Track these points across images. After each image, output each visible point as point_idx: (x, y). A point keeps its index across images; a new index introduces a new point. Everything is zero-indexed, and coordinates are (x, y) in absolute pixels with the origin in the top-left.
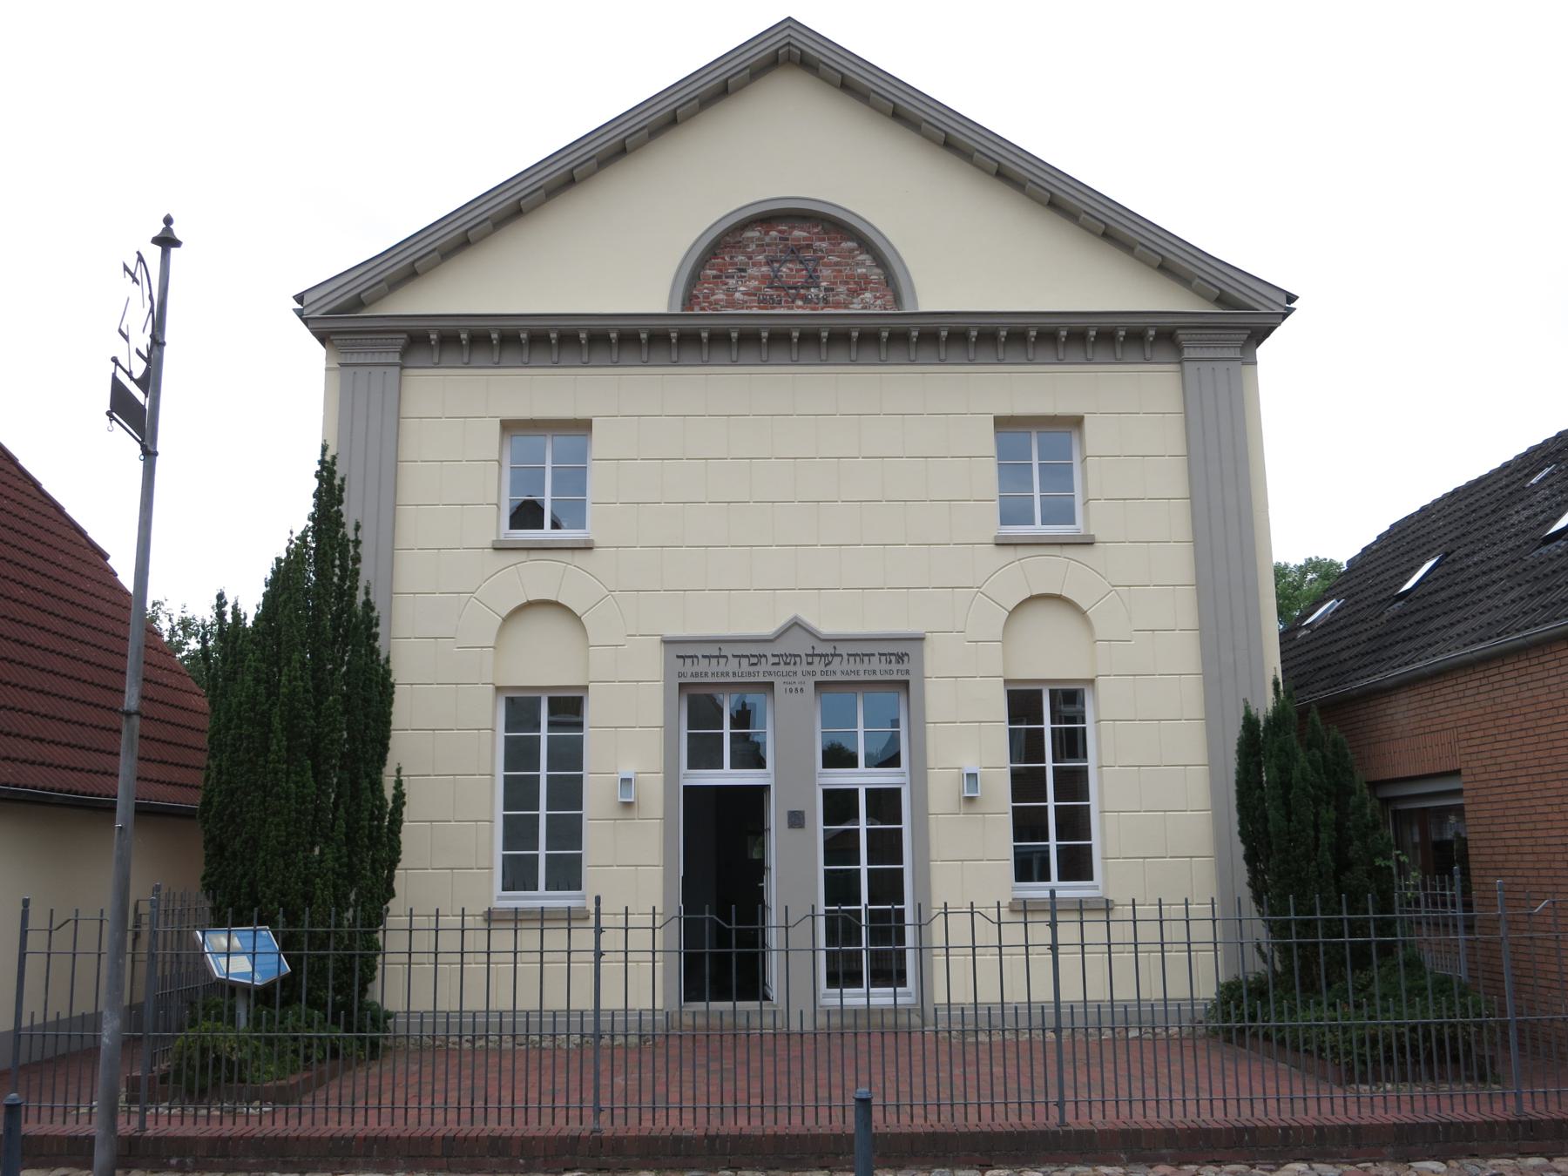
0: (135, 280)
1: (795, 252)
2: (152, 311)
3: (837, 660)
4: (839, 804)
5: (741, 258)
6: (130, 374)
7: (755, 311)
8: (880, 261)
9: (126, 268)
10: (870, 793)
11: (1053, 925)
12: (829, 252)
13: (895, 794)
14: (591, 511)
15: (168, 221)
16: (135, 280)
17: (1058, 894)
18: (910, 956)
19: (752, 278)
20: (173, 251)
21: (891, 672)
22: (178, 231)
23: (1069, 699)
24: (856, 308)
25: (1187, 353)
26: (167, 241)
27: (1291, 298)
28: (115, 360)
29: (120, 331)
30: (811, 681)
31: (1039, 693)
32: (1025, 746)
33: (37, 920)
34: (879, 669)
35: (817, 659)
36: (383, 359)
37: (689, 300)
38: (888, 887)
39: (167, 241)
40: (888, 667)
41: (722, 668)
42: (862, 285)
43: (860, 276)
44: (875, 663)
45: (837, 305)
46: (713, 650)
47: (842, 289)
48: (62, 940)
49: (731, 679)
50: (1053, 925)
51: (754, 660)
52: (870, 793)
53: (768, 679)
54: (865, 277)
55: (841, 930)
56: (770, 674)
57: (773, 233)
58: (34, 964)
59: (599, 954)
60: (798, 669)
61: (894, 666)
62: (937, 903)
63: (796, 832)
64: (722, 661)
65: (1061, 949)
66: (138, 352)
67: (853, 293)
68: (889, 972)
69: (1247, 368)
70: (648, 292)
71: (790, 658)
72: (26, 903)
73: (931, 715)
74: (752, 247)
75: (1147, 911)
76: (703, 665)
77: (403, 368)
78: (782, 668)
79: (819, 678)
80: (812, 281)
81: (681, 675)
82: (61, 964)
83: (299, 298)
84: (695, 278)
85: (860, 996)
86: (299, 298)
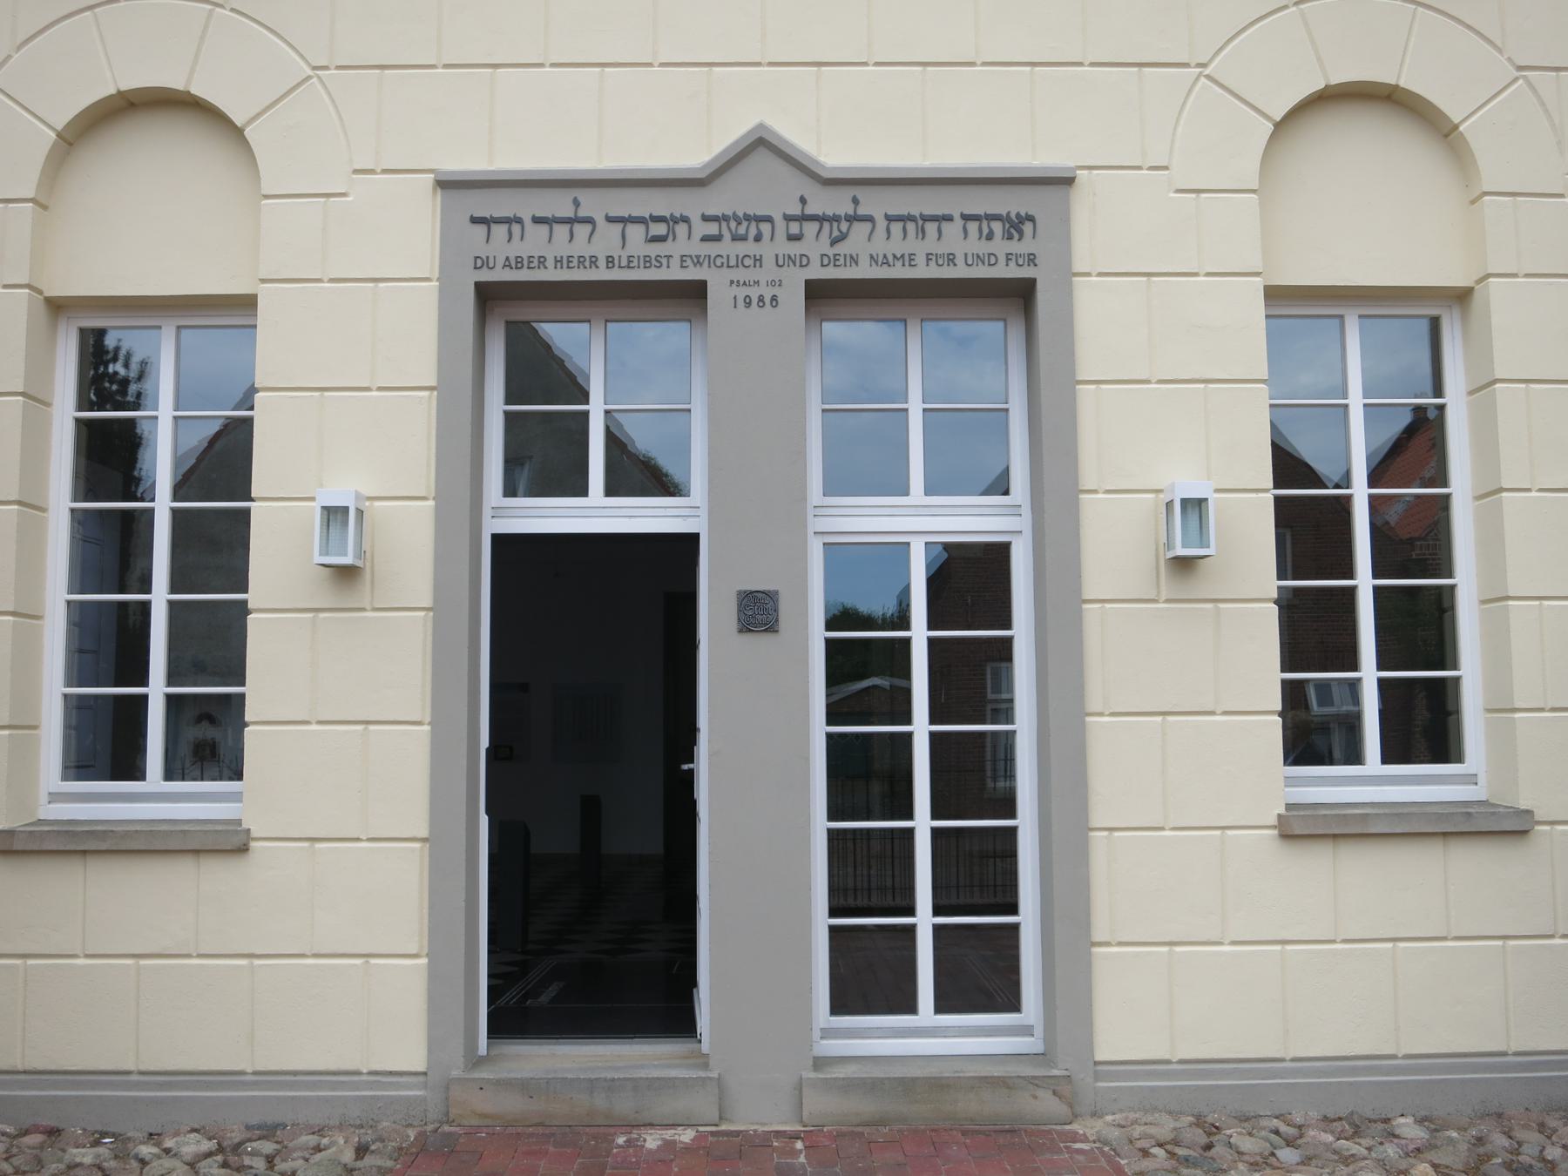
3: (861, 229)
13: (995, 558)
21: (990, 259)
34: (963, 255)
35: (810, 228)
40: (984, 247)
41: (580, 247)
46: (559, 204)
49: (602, 274)
51: (659, 229)
53: (692, 274)
55: (866, 875)
56: (698, 262)
60: (767, 250)
61: (1000, 246)
64: (582, 231)
68: (982, 975)
73: (1089, 362)
76: (534, 241)
78: (727, 248)
79: (817, 272)
81: (481, 263)
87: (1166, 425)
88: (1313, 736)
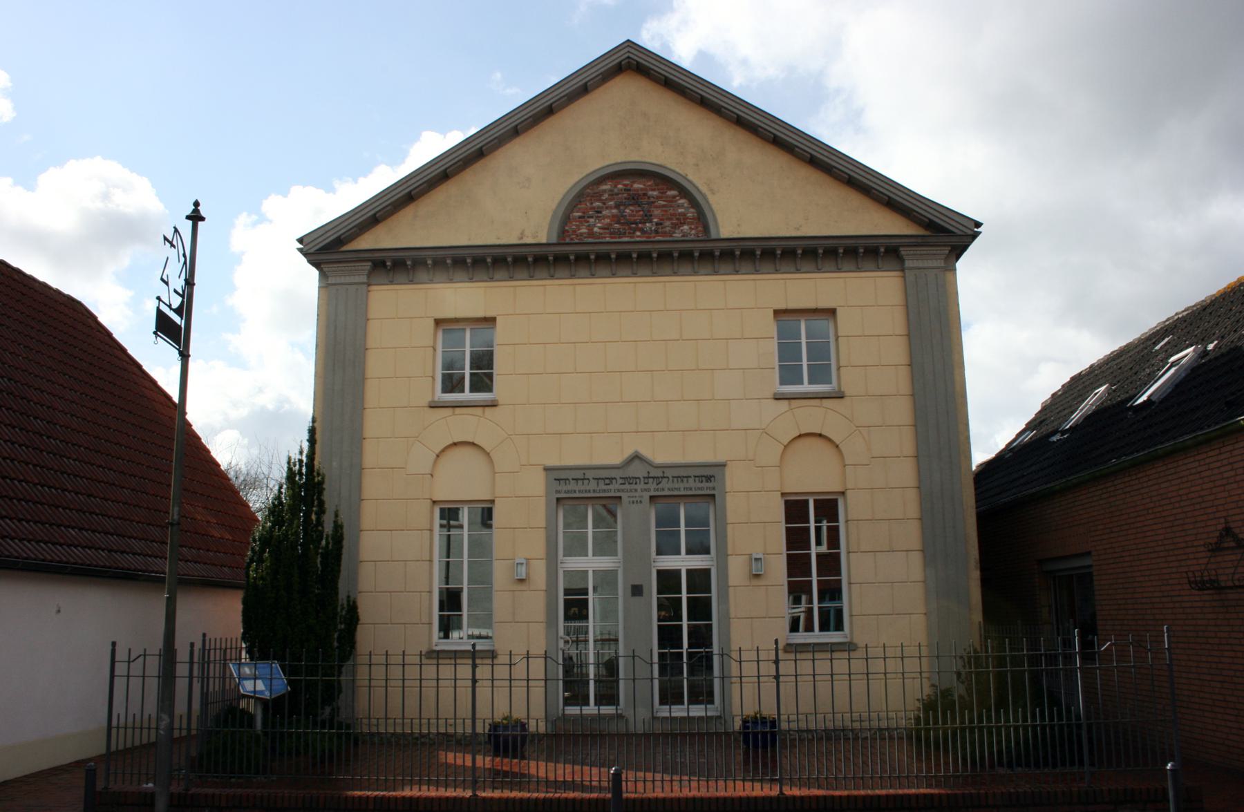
0: (172, 245)
1: (635, 199)
2: (185, 263)
3: (665, 480)
4: (668, 580)
5: (597, 204)
6: (170, 306)
7: (608, 239)
8: (694, 203)
9: (165, 239)
10: (689, 572)
11: (474, 666)
12: (658, 198)
13: (706, 573)
14: (497, 379)
15: (196, 204)
16: (172, 245)
17: (478, 648)
18: (717, 683)
19: (605, 217)
20: (200, 223)
21: (702, 489)
22: (203, 211)
23: (828, 508)
24: (677, 235)
25: (908, 264)
26: (196, 217)
27: (978, 225)
28: (159, 298)
29: (162, 279)
30: (646, 495)
31: (807, 502)
32: (796, 539)
33: (121, 655)
34: (694, 486)
36: (357, 279)
37: (563, 232)
38: (701, 637)
39: (196, 217)
42: (682, 220)
43: (680, 214)
44: (691, 483)
45: (664, 234)
46: (579, 475)
47: (668, 223)
48: (136, 668)
50: (474, 666)
52: (689, 572)
53: (618, 494)
54: (684, 214)
57: (620, 186)
58: (120, 683)
59: (474, 681)
60: (639, 487)
61: (705, 485)
62: (735, 647)
63: (637, 599)
65: (781, 679)
66: (175, 291)
67: (675, 226)
68: (702, 694)
69: (949, 274)
72: (114, 644)
73: (731, 517)
74: (606, 196)
75: (875, 652)
76: (572, 486)
77: (369, 285)
78: (627, 486)
80: (648, 217)
81: (558, 492)
82: (135, 683)
83: (300, 241)
84: (567, 219)
85: (682, 710)
86: (300, 241)
87: (752, 534)
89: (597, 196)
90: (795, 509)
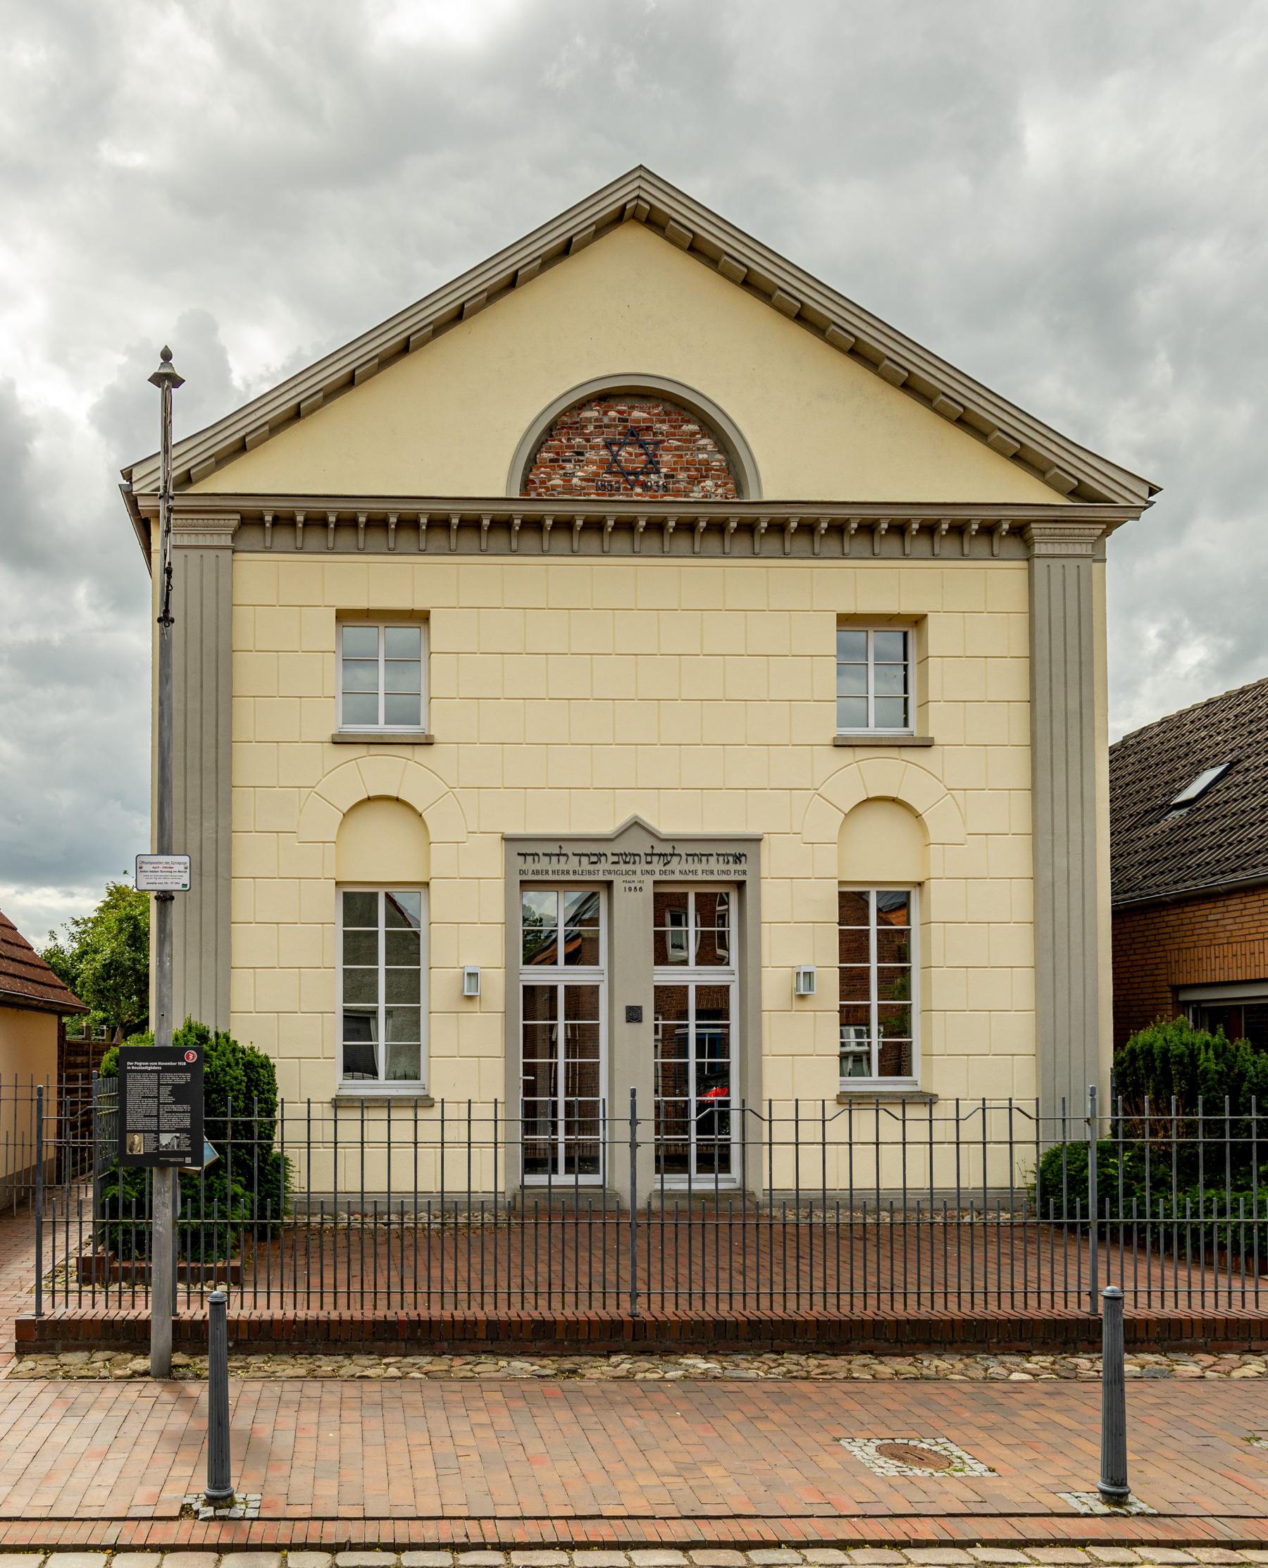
1: (634, 434)
3: (676, 859)
7: (593, 497)
8: (724, 444)
24: (697, 495)
25: (1039, 549)
30: (649, 880)
35: (655, 859)
37: (527, 484)
40: (725, 867)
41: (563, 866)
42: (704, 471)
45: (678, 492)
47: (682, 476)
49: (571, 877)
51: (594, 859)
54: (706, 463)
56: (610, 872)
57: (612, 414)
60: (638, 868)
63: (634, 1026)
64: (563, 859)
67: (693, 481)
70: (484, 471)
71: (627, 857)
74: (591, 428)
76: (544, 864)
79: (658, 877)
80: (652, 465)
81: (522, 872)
88: (854, 1062)
89: (578, 428)
90: (852, 903)
